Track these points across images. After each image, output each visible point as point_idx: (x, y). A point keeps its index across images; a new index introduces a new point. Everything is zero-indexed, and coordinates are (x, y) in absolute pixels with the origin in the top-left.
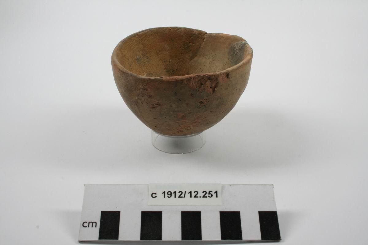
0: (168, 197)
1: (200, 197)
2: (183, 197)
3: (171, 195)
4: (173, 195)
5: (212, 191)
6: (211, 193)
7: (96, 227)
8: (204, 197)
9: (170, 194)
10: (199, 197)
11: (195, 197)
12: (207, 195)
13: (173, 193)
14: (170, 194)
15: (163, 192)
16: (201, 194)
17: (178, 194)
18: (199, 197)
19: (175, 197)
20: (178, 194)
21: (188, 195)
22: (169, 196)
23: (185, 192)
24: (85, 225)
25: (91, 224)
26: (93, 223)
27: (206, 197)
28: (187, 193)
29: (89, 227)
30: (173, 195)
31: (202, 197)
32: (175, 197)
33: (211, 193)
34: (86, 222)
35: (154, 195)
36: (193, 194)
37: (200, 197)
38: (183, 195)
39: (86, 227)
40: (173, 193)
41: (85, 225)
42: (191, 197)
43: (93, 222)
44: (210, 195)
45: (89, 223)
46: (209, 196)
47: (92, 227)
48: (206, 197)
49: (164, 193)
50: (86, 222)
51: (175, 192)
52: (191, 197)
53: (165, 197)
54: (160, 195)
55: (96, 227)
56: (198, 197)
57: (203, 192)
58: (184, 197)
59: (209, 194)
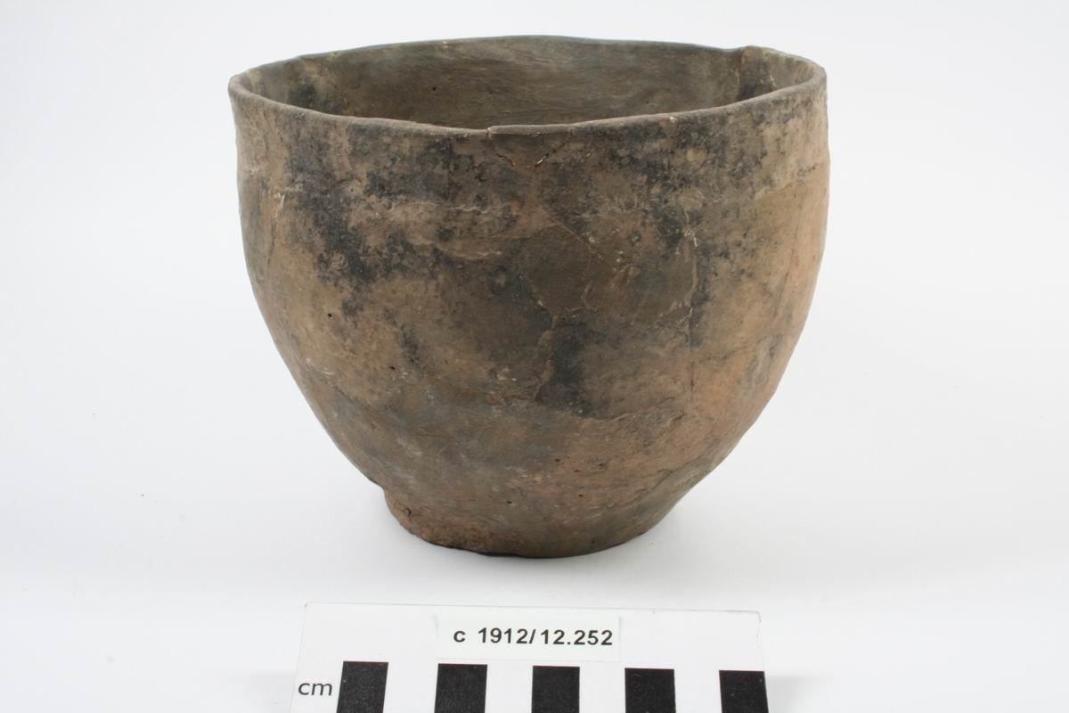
0: (492, 640)
1: (569, 643)
2: (528, 641)
3: (499, 636)
4: (505, 637)
5: (596, 632)
6: (594, 634)
7: (330, 694)
8: (577, 643)
10: (566, 643)
11: (556, 642)
12: (586, 639)
16: (570, 637)
17: (515, 636)
18: (566, 643)
19: (509, 641)
20: (515, 636)
21: (539, 638)
22: (496, 639)
23: (534, 631)
24: (304, 689)
25: (318, 689)
26: (322, 687)
27: (584, 644)
29: (313, 694)
30: (505, 637)
31: (573, 642)
32: (509, 641)
33: (594, 634)
34: (308, 684)
35: (460, 637)
36: (553, 637)
37: (569, 643)
38: (527, 639)
41: (304, 689)
42: (546, 642)
44: (593, 640)
45: (314, 685)
46: (589, 642)
47: (321, 694)
48: (584, 644)
49: (484, 631)
50: (308, 684)
51: (509, 632)
52: (546, 642)
53: (484, 641)
54: (473, 637)
55: (330, 694)
56: (563, 643)
57: (576, 633)
58: (531, 642)
59: (590, 636)
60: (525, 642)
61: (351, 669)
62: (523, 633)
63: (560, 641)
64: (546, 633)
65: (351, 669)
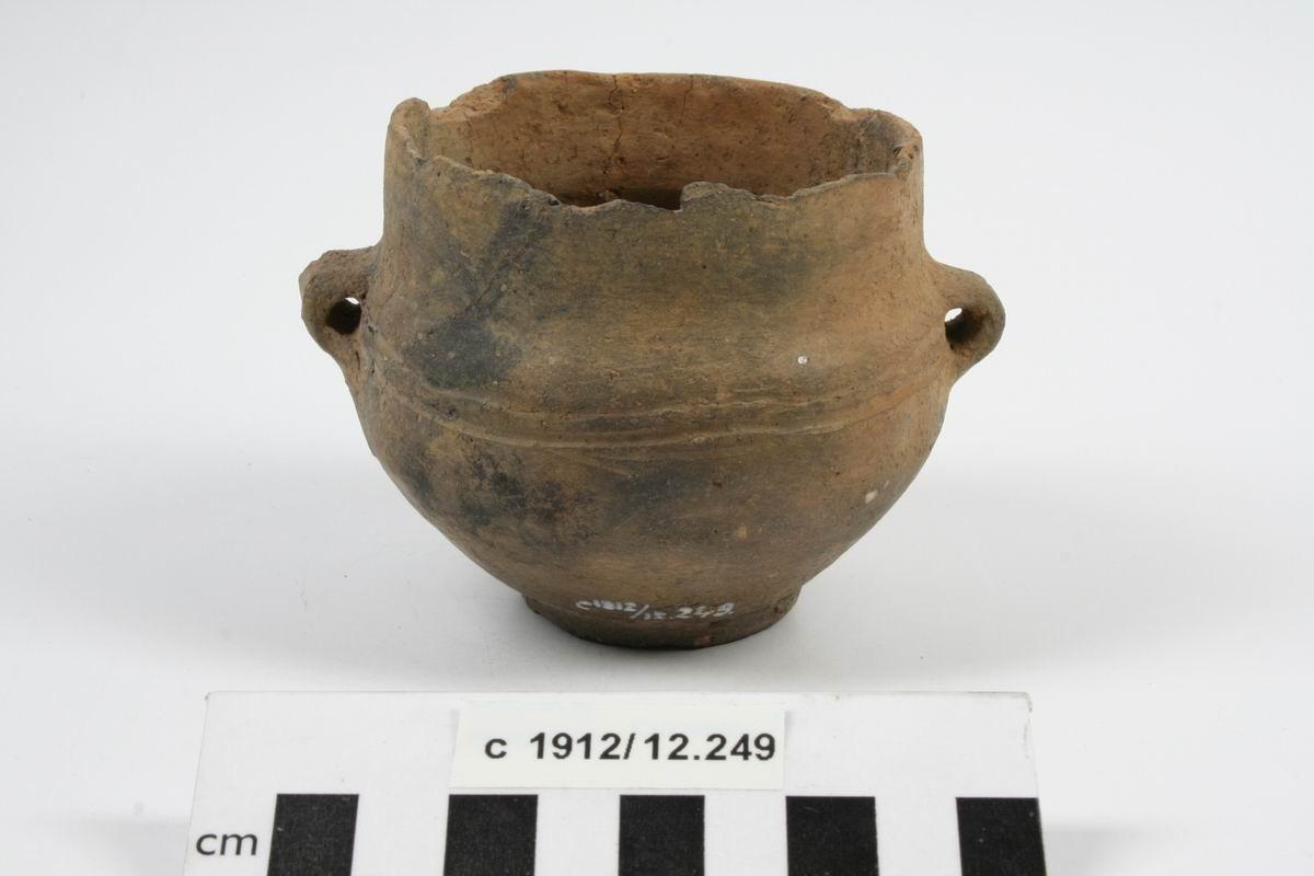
0: (557, 755)
1: (697, 758)
2: (622, 755)
3: (568, 747)
4: (578, 749)
7: (254, 852)
8: (711, 756)
9: (564, 745)
10: (691, 757)
11: (673, 756)
13: (579, 741)
14: (564, 745)
15: (533, 736)
16: (699, 746)
17: (598, 747)
18: (691, 757)
19: (587, 755)
20: (598, 747)
21: (642, 750)
22: (562, 752)
23: (632, 737)
24: (207, 845)
25: (232, 843)
26: (240, 839)
28: (639, 744)
29: (223, 852)
30: (578, 749)
32: (587, 755)
34: (214, 837)
35: (496, 749)
36: (666, 747)
37: (697, 758)
38: (620, 750)
39: (212, 853)
40: (579, 741)
41: (207, 845)
42: (655, 756)
43: (242, 836)
45: (225, 838)
47: (238, 852)
49: (540, 738)
50: (214, 837)
51: (587, 739)
52: (655, 756)
53: (540, 755)
54: (521, 750)
55: (254, 852)
56: (685, 758)
57: (711, 738)
58: (627, 756)
60: (617, 757)
61: (291, 808)
62: (611, 741)
63: (679, 754)
64: (654, 739)
65: (291, 808)
